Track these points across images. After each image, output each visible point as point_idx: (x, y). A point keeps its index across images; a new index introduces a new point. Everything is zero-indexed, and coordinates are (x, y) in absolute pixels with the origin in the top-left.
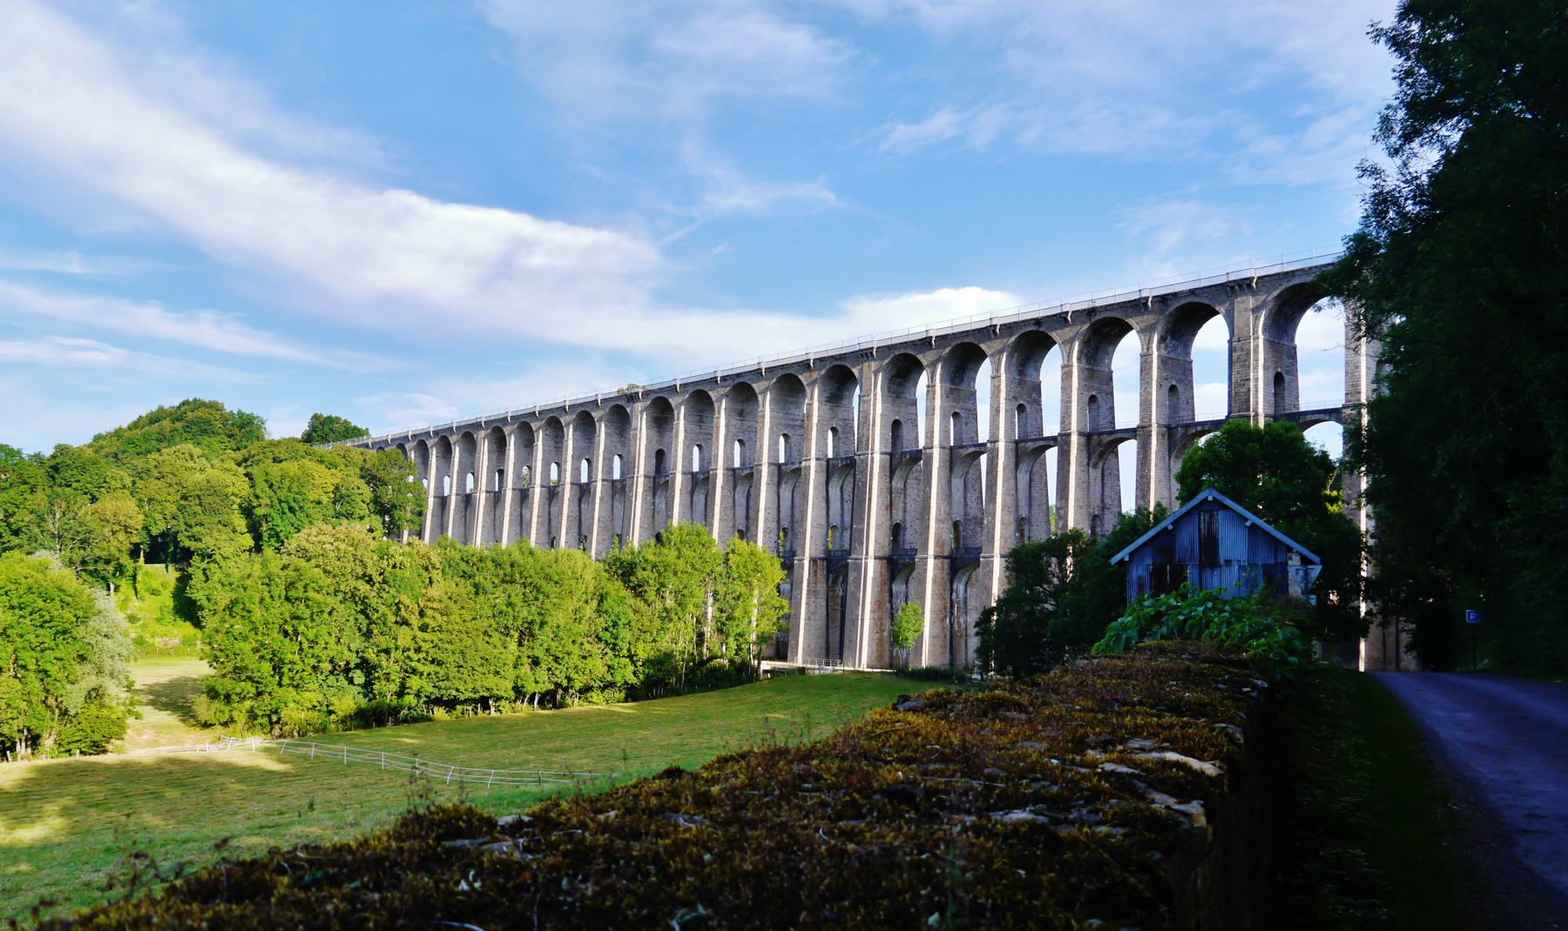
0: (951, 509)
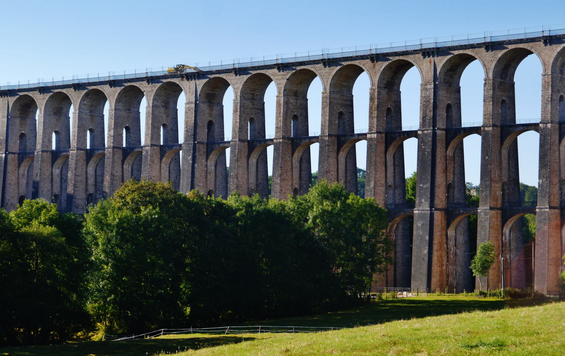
0: (501, 173)
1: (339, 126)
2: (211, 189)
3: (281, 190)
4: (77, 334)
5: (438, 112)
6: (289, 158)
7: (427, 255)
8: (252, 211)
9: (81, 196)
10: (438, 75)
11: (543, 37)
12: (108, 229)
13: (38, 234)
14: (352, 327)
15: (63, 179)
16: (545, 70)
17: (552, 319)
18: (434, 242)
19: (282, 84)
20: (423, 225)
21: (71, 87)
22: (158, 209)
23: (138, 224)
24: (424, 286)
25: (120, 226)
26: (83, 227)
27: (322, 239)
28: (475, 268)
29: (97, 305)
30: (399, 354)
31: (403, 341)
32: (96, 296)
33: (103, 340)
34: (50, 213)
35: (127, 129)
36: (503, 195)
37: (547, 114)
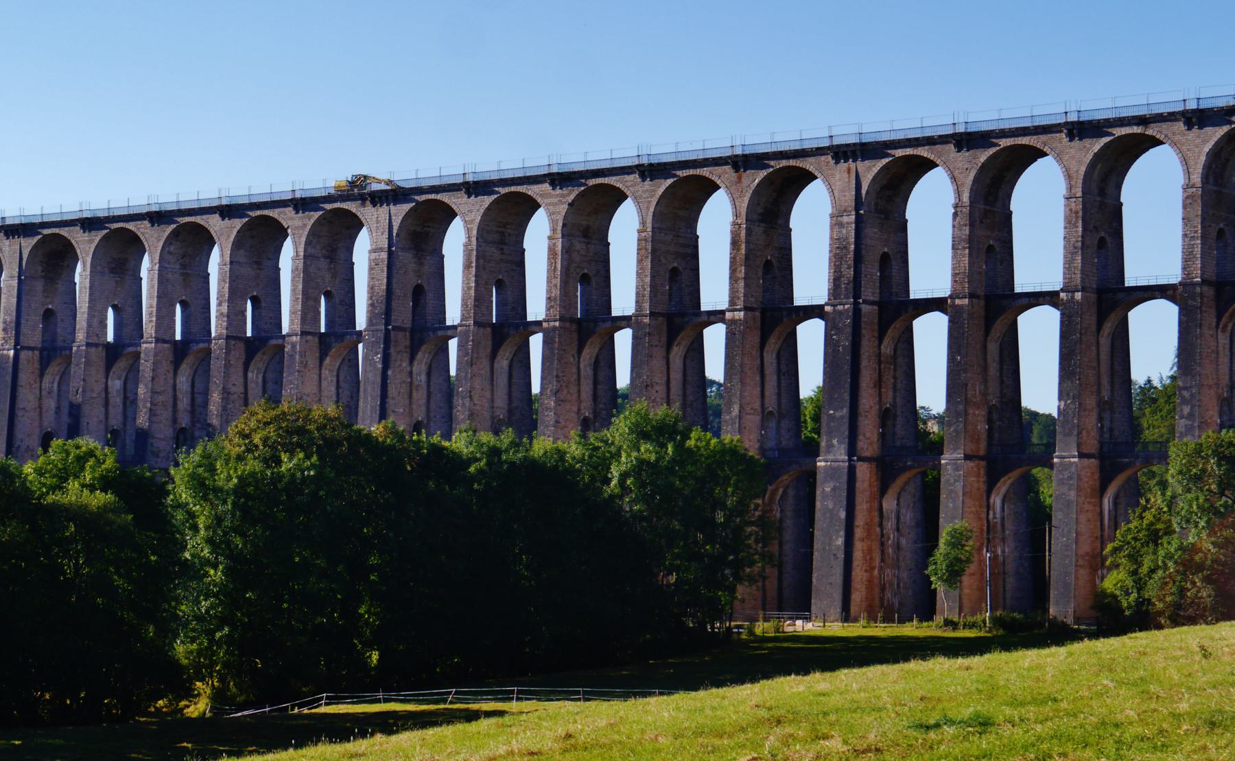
0: (986, 388)
1: (670, 295)
2: (420, 419)
3: (557, 422)
4: (156, 703)
5: (863, 269)
6: (572, 360)
7: (843, 548)
8: (501, 462)
9: (163, 432)
10: (864, 196)
11: (1067, 123)
12: (218, 498)
13: (80, 507)
14: (696, 689)
15: (129, 400)
16: (1070, 188)
17: (1084, 672)
18: (857, 523)
19: (559, 213)
20: (834, 489)
21: (145, 219)
22: (314, 458)
23: (276, 488)
24: (836, 609)
25: (239, 491)
26: (168, 493)
27: (637, 517)
28: (936, 574)
29: (195, 646)
30: (787, 741)
31: (795, 717)
32: (193, 630)
33: (208, 715)
34: (103, 466)
35: (255, 302)
36: (990, 432)
37: (1074, 273)
